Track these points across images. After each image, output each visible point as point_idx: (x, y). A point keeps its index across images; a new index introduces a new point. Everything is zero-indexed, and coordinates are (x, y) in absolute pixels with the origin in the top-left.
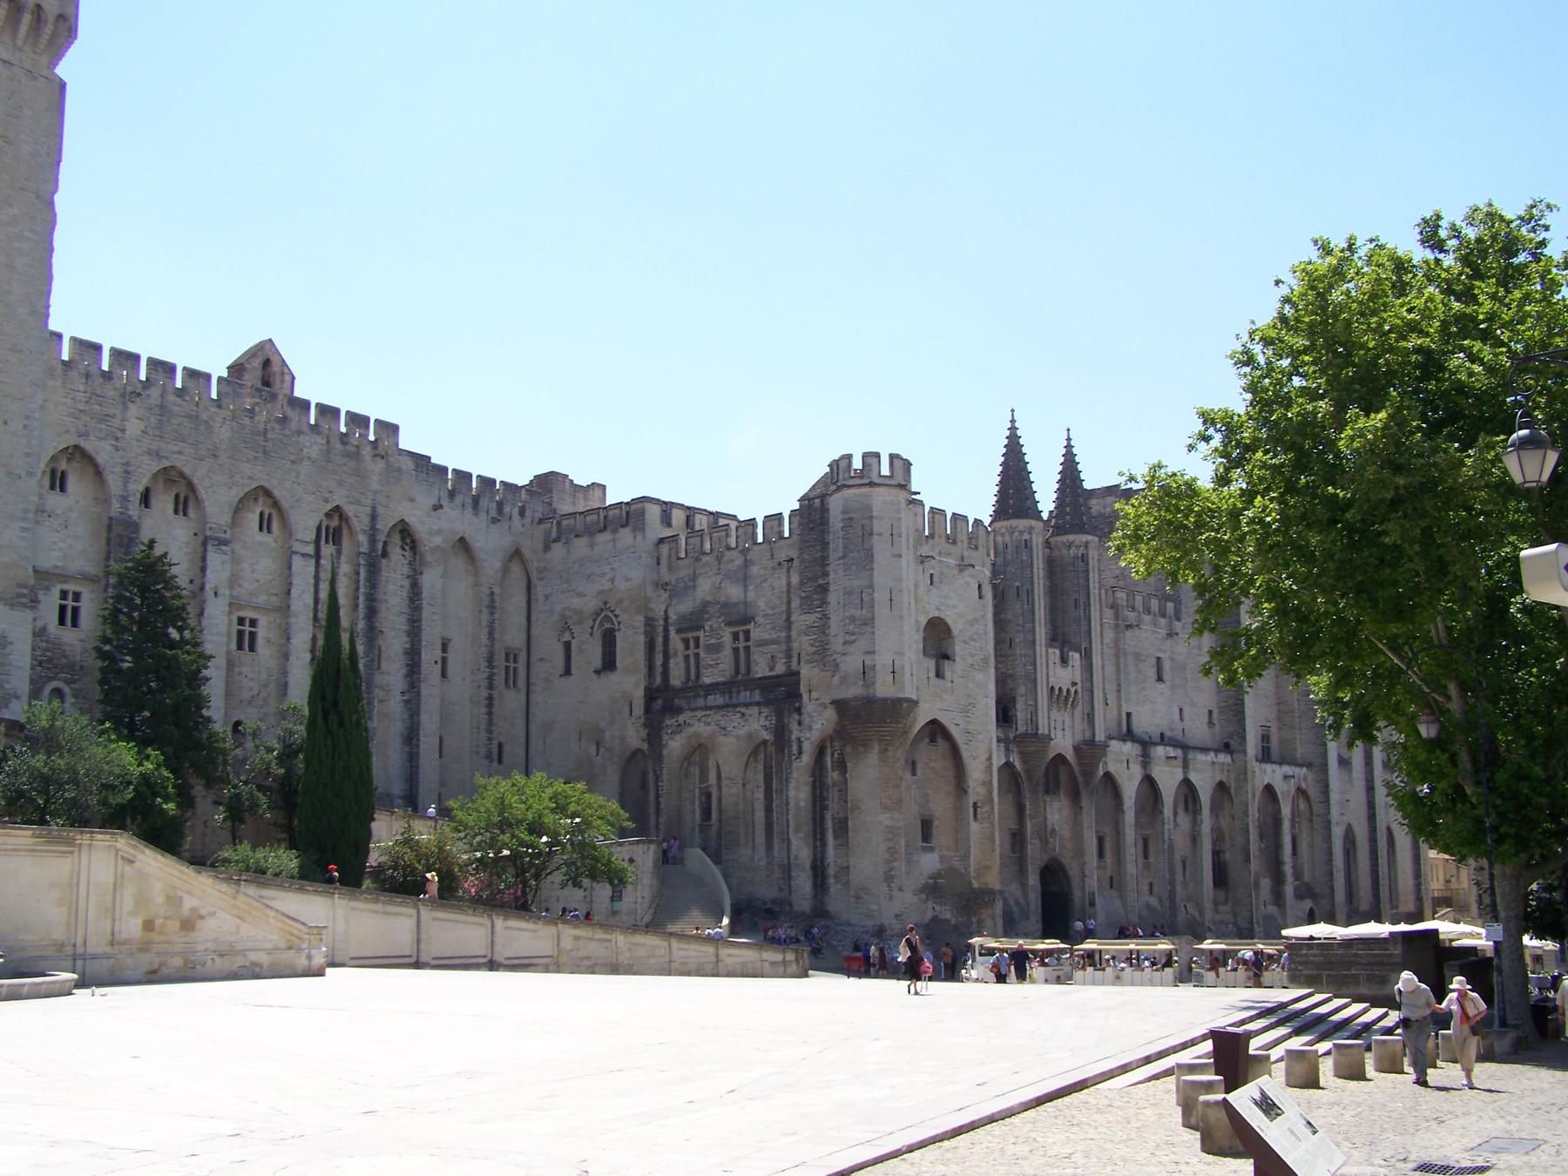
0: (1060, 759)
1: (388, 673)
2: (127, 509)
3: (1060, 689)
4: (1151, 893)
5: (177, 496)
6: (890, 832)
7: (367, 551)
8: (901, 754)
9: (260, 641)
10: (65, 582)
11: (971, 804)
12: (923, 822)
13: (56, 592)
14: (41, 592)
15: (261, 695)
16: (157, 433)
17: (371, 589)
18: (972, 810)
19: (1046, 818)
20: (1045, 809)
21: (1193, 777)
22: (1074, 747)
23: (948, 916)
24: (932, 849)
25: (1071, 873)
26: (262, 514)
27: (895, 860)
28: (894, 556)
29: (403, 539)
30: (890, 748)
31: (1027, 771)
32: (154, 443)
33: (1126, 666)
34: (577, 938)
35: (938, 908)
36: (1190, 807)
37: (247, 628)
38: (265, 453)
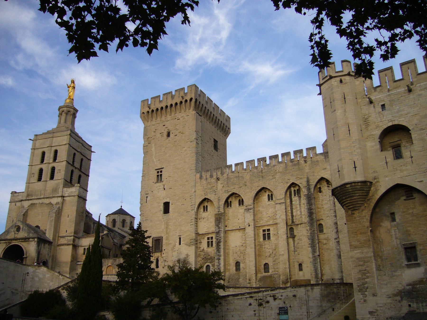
1: (327, 233)
2: (220, 210)
5: (240, 200)
7: (307, 194)
8: (366, 213)
9: (271, 236)
10: (208, 235)
12: (406, 249)
13: (206, 238)
14: (202, 240)
15: (274, 253)
16: (227, 186)
17: (310, 206)
24: (418, 265)
26: (269, 195)
27: (368, 277)
28: (332, 112)
29: (328, 184)
32: (226, 189)
37: (266, 232)
38: (262, 177)
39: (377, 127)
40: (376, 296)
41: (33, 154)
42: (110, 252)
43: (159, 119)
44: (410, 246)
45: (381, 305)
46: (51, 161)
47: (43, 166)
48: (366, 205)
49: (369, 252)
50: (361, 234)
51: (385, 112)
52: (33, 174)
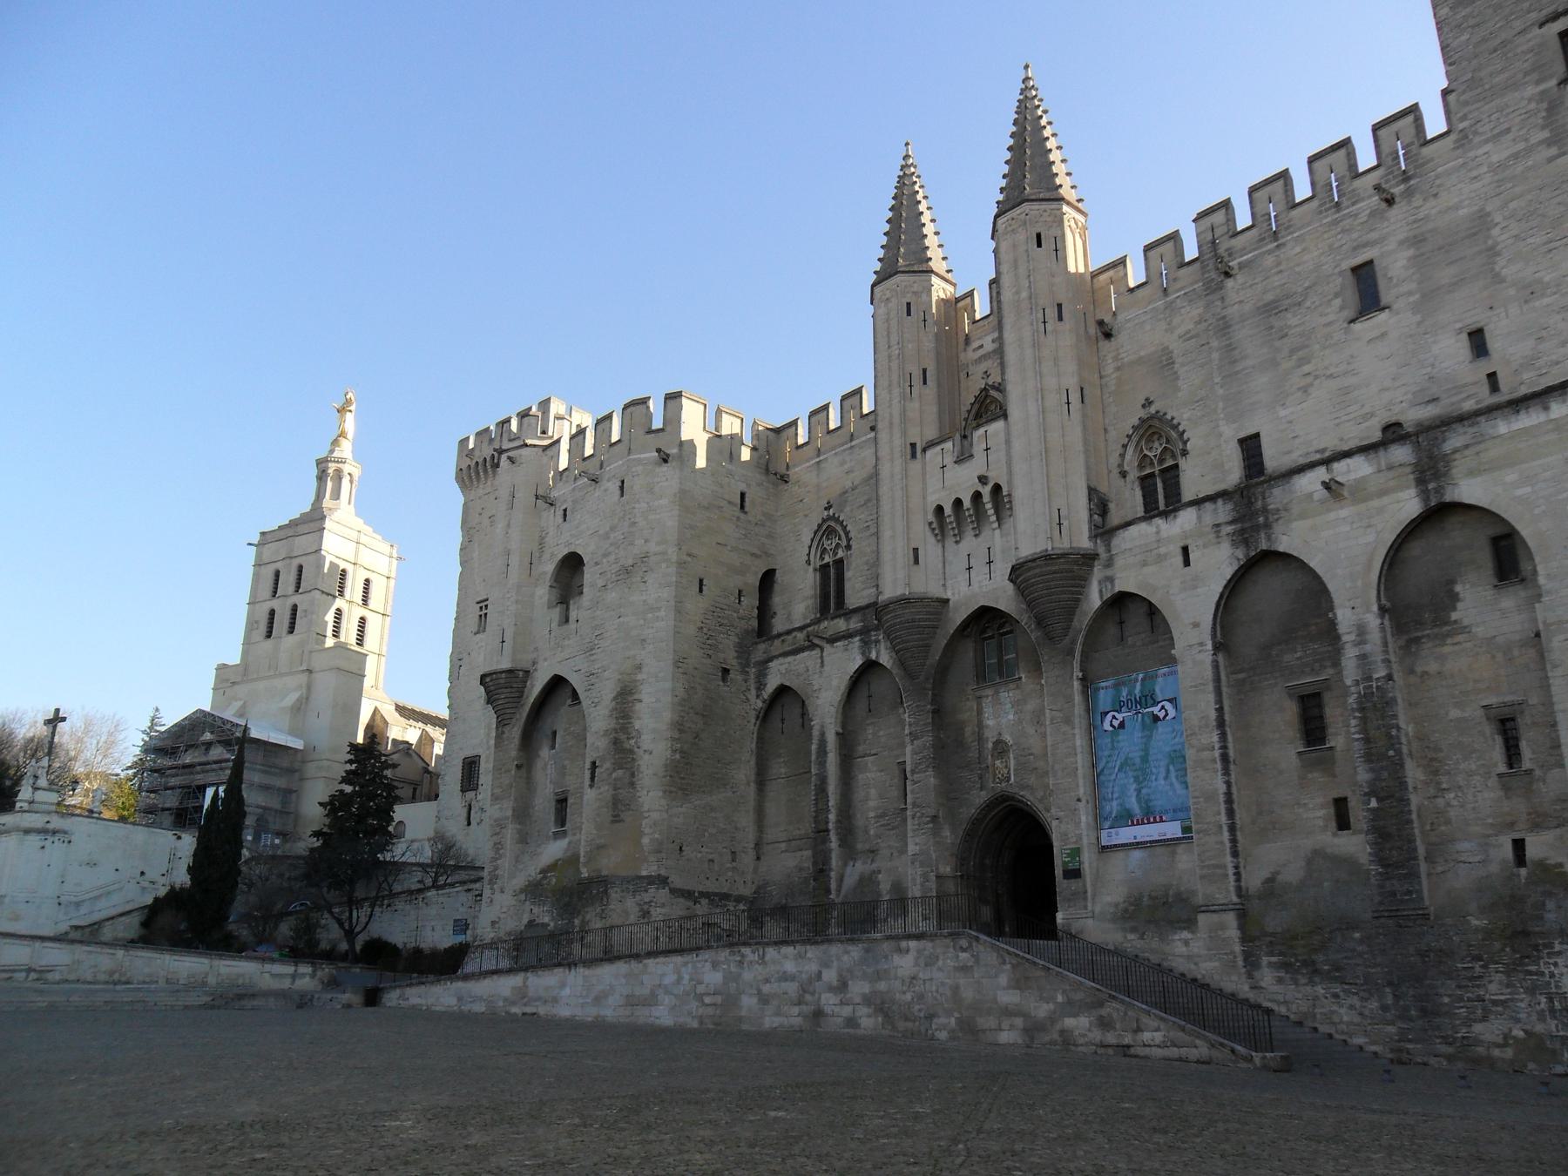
0: (985, 619)
3: (958, 503)
4: (1343, 823)
6: (498, 825)
11: (588, 765)
18: (587, 774)
19: (980, 725)
20: (980, 712)
21: (1468, 489)
22: (1011, 580)
23: (546, 920)
25: (1047, 815)
30: (506, 729)
31: (902, 663)
33: (1229, 348)
34: (90, 952)
35: (536, 910)
36: (1525, 567)
39: (552, 555)
40: (503, 892)
41: (256, 578)
42: (415, 789)
43: (489, 483)
44: (562, 797)
45: (504, 910)
46: (292, 589)
47: (275, 604)
48: (518, 716)
49: (507, 808)
50: (505, 772)
51: (566, 525)
52: (256, 622)
